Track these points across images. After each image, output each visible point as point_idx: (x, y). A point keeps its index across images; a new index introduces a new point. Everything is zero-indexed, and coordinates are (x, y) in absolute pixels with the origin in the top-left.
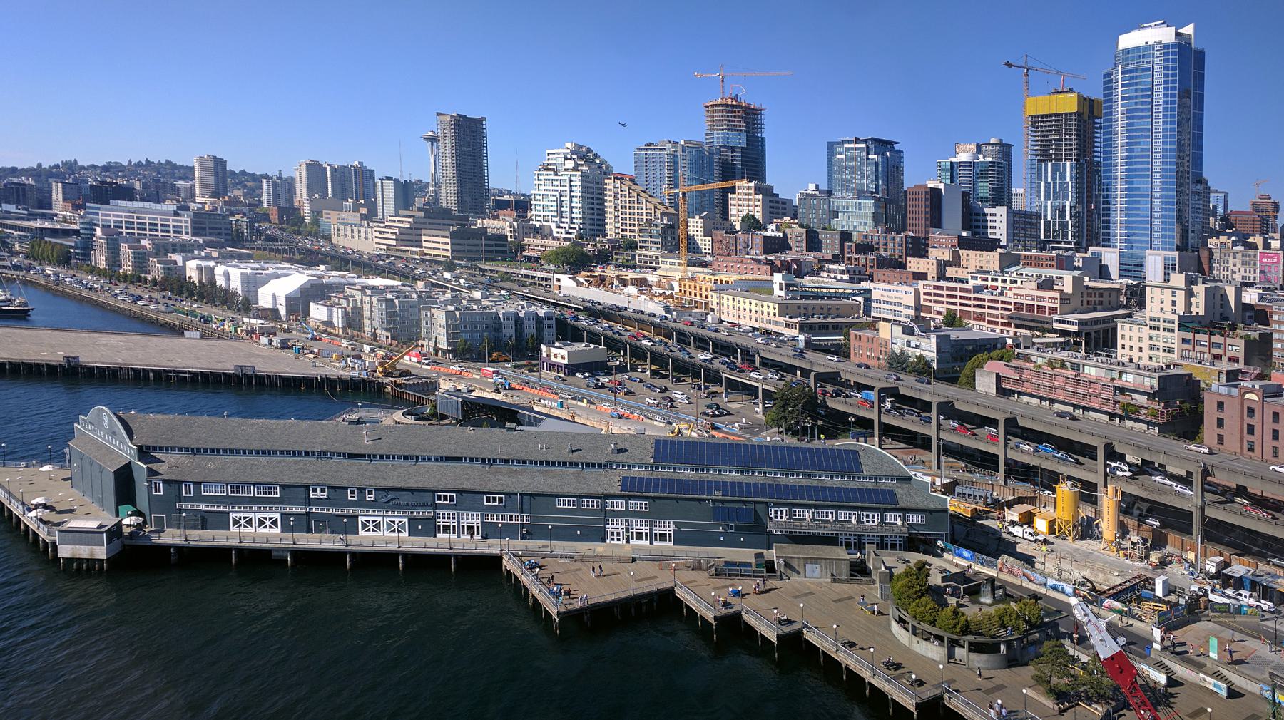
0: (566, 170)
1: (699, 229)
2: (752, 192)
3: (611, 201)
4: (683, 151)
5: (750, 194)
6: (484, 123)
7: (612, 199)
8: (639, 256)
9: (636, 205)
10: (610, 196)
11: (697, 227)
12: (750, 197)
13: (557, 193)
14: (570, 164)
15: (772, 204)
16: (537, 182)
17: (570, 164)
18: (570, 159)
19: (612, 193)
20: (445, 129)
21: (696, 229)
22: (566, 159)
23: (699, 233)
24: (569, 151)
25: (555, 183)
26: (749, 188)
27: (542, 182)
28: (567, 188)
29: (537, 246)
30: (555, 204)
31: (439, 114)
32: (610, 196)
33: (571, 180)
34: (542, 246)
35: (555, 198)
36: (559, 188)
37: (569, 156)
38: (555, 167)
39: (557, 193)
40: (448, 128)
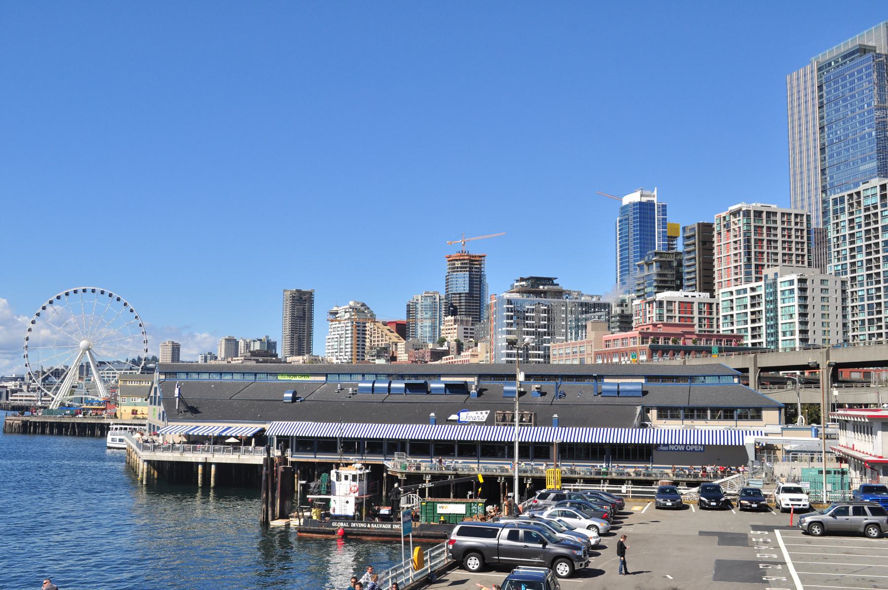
0: (345, 320)
2: (452, 323)
5: (452, 325)
12: (452, 327)
13: (338, 336)
15: (466, 331)
16: (330, 330)
17: (347, 315)
22: (346, 312)
25: (339, 329)
26: (452, 320)
28: (343, 332)
30: (336, 343)
35: (337, 340)
36: (340, 332)
37: (347, 310)
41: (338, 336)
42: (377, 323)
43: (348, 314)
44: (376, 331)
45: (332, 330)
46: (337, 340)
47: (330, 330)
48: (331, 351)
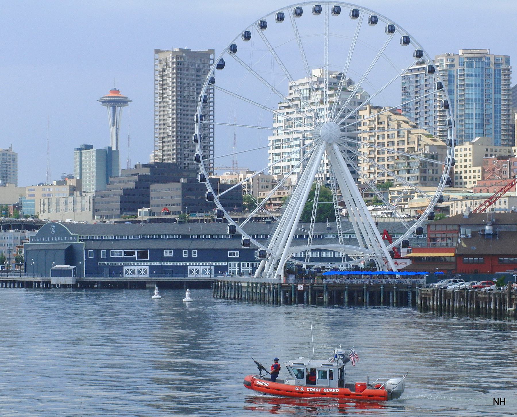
1: (468, 158)
3: (365, 139)
4: (461, 64)
6: (211, 56)
7: (366, 135)
8: (392, 193)
9: (396, 140)
10: (365, 131)
11: (465, 155)
14: (317, 96)
16: (275, 125)
17: (317, 96)
18: (317, 89)
19: (366, 128)
20: (164, 70)
21: (463, 158)
23: (468, 163)
24: (315, 79)
27: (282, 124)
29: (275, 199)
31: (157, 51)
32: (365, 131)
33: (317, 116)
34: (280, 199)
35: (297, 143)
38: (298, 102)
39: (300, 136)
40: (169, 69)
41: (300, 136)
42: (382, 111)
43: (319, 93)
44: (386, 126)
45: (282, 124)
46: (297, 143)
47: (275, 125)
48: (281, 164)
